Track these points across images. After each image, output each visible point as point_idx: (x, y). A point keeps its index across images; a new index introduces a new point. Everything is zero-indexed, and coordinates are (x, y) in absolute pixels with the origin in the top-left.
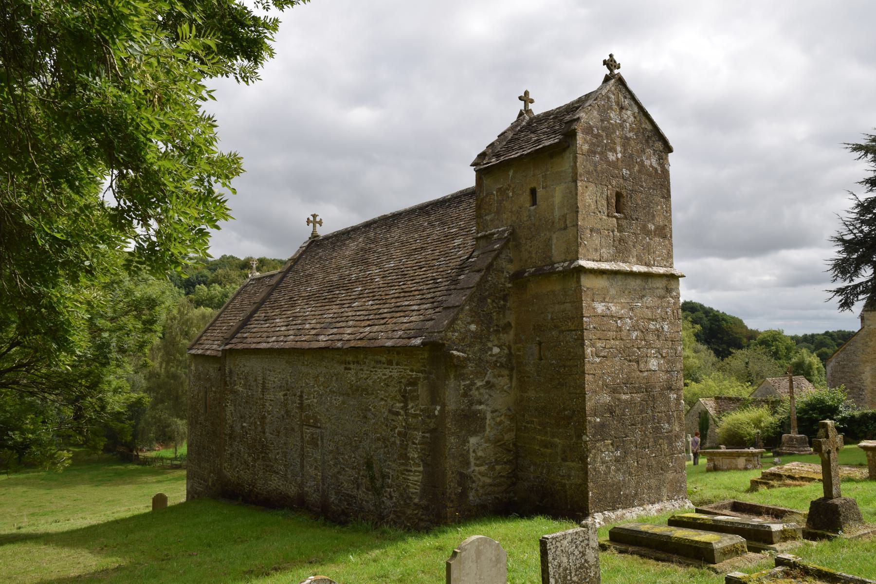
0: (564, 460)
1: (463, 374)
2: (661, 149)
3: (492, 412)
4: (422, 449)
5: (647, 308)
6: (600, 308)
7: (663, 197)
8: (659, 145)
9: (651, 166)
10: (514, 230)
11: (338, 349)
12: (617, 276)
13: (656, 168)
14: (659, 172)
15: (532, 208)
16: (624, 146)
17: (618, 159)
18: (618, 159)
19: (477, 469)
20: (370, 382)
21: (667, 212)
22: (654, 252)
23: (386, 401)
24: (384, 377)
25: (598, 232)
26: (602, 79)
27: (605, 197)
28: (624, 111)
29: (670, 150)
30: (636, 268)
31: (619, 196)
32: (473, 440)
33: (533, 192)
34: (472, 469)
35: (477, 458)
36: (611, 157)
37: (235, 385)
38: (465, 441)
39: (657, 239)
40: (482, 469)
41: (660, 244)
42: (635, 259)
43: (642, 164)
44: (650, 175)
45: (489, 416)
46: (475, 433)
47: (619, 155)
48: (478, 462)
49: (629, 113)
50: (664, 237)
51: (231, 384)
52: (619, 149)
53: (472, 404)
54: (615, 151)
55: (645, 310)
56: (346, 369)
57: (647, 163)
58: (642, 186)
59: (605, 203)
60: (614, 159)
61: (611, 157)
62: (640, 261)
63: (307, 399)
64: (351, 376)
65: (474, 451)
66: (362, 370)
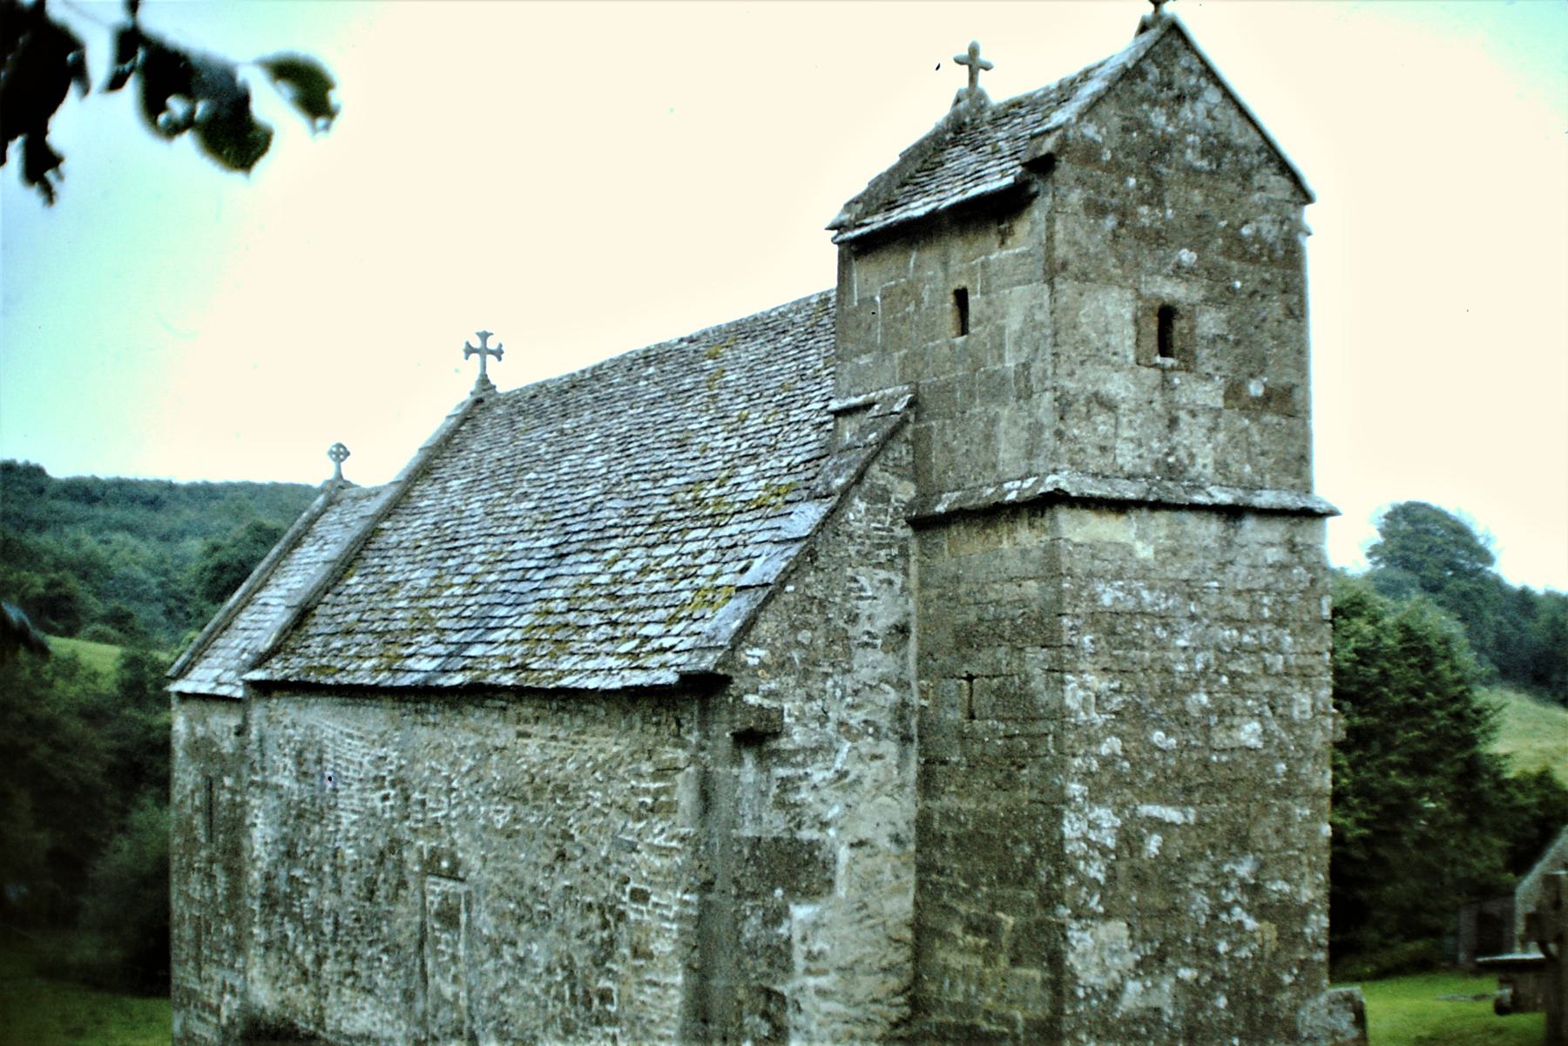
0: (1015, 961)
1: (776, 752)
3: (852, 845)
4: (682, 932)
5: (1238, 594)
6: (1108, 596)
8: (1279, 187)
10: (916, 393)
11: (506, 688)
12: (1157, 514)
15: (960, 340)
19: (811, 981)
20: (571, 767)
23: (605, 815)
24: (601, 757)
26: (1136, 26)
29: (1307, 198)
32: (802, 912)
33: (961, 297)
34: (797, 983)
35: (810, 956)
37: (272, 775)
38: (778, 916)
40: (823, 982)
45: (844, 854)
46: (810, 895)
48: (813, 966)
51: (263, 769)
53: (799, 826)
55: (1233, 601)
56: (521, 735)
63: (434, 810)
64: (532, 749)
65: (804, 939)
66: (554, 738)
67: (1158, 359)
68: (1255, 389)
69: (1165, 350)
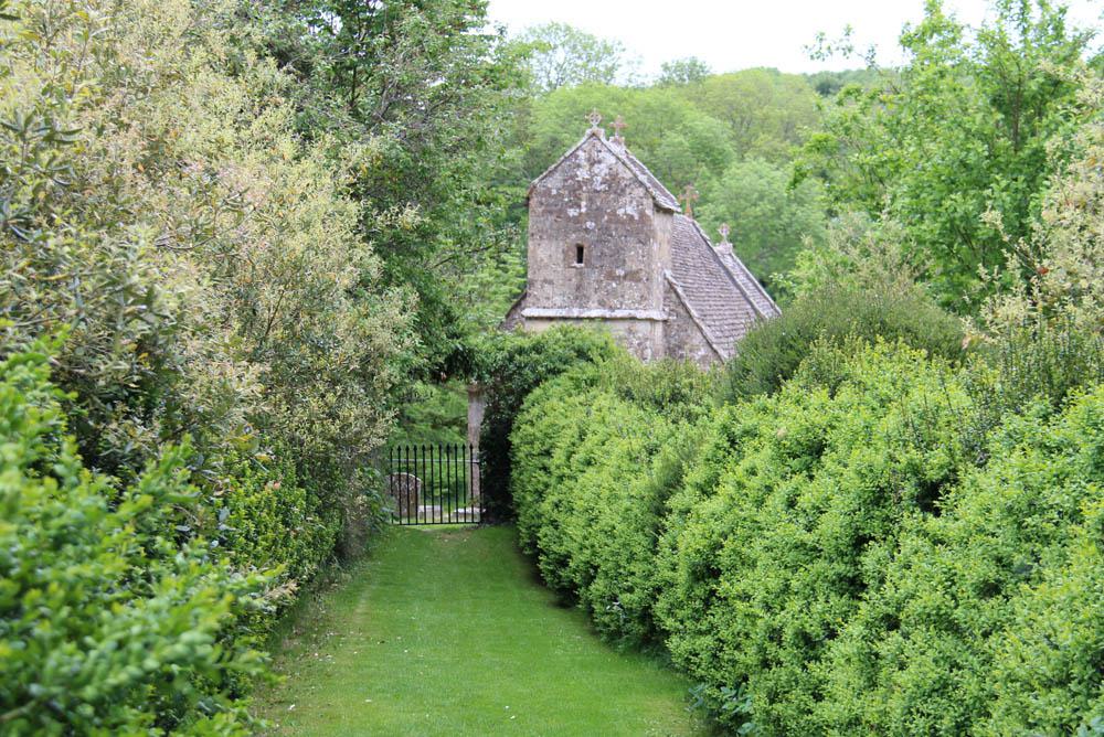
2: (642, 195)
7: (640, 242)
9: (625, 214)
13: (632, 217)
14: (636, 218)
16: (591, 200)
17: (580, 214)
18: (580, 214)
21: (643, 256)
22: (623, 296)
25: (551, 282)
27: (560, 250)
28: (596, 165)
30: (594, 313)
31: (580, 250)
36: (572, 212)
39: (627, 283)
41: (631, 287)
42: (596, 304)
43: (614, 213)
44: (623, 223)
47: (583, 210)
49: (602, 166)
50: (640, 280)
52: (583, 203)
54: (579, 207)
57: (620, 212)
58: (611, 235)
59: (561, 256)
60: (576, 214)
61: (572, 212)
62: (602, 304)
67: (575, 264)
68: (620, 272)
69: (580, 261)
